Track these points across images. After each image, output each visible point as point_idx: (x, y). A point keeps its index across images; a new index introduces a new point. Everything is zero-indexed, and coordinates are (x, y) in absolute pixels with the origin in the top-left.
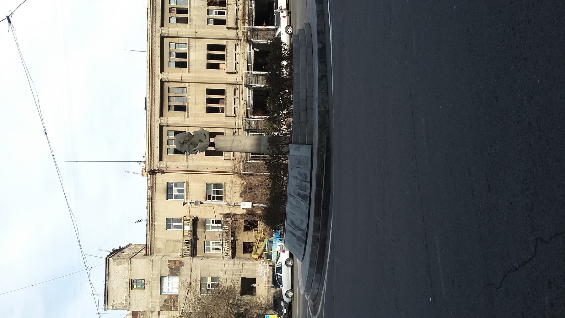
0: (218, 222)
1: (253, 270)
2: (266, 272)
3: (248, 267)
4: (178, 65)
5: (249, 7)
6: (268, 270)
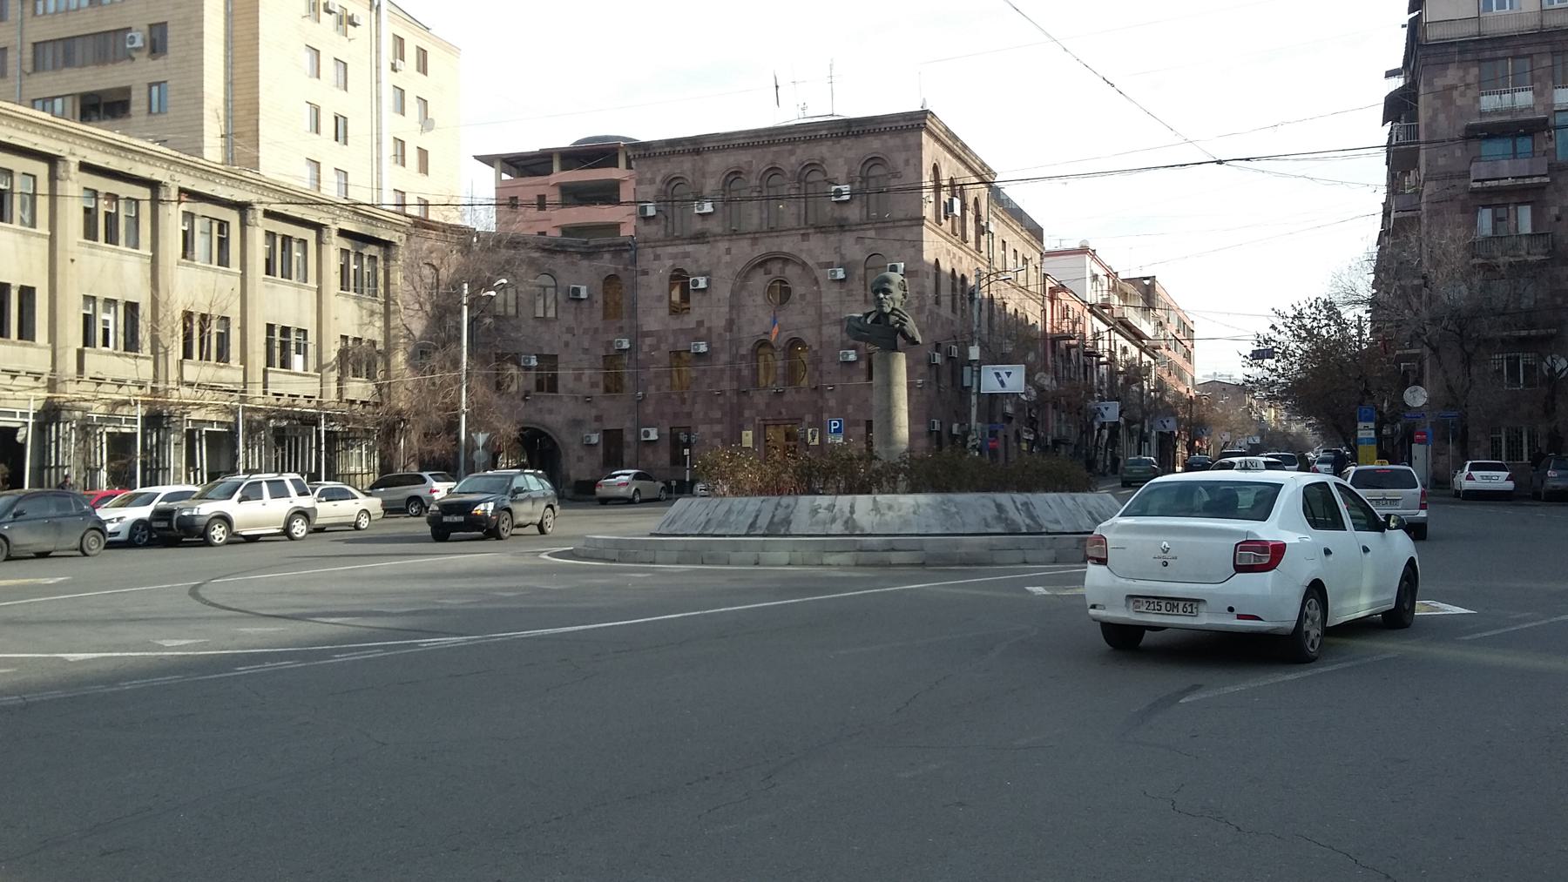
5: (124, 418)
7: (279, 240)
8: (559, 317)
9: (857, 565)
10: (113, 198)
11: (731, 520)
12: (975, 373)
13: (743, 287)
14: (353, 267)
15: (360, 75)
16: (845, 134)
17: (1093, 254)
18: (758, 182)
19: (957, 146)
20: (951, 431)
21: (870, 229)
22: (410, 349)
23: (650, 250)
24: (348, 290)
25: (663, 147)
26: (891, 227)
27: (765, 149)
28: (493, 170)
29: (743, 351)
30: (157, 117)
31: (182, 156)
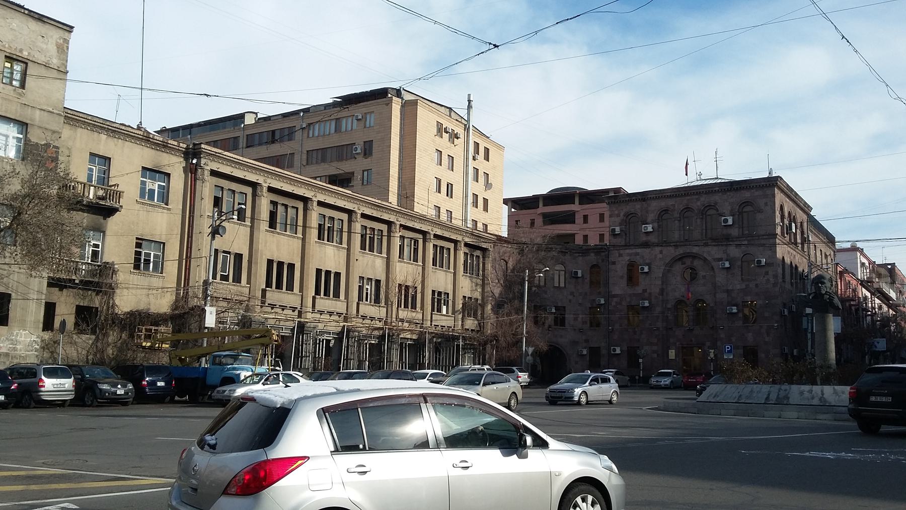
0: (95, 254)
1: (25, 321)
2: (19, 349)
3: (32, 311)
4: (321, 227)
6: (23, 353)
7: (438, 248)
8: (567, 287)
9: (835, 420)
10: (373, 229)
11: (754, 396)
12: (810, 321)
13: (669, 271)
14: (469, 261)
15: (459, 163)
16: (729, 189)
17: (862, 251)
18: (678, 216)
19: (792, 194)
20: (793, 353)
21: (745, 240)
22: (493, 303)
23: (616, 251)
24: (467, 273)
25: (623, 198)
26: (757, 239)
27: (683, 198)
28: (507, 207)
29: (669, 306)
30: (366, 186)
31: (402, 209)
